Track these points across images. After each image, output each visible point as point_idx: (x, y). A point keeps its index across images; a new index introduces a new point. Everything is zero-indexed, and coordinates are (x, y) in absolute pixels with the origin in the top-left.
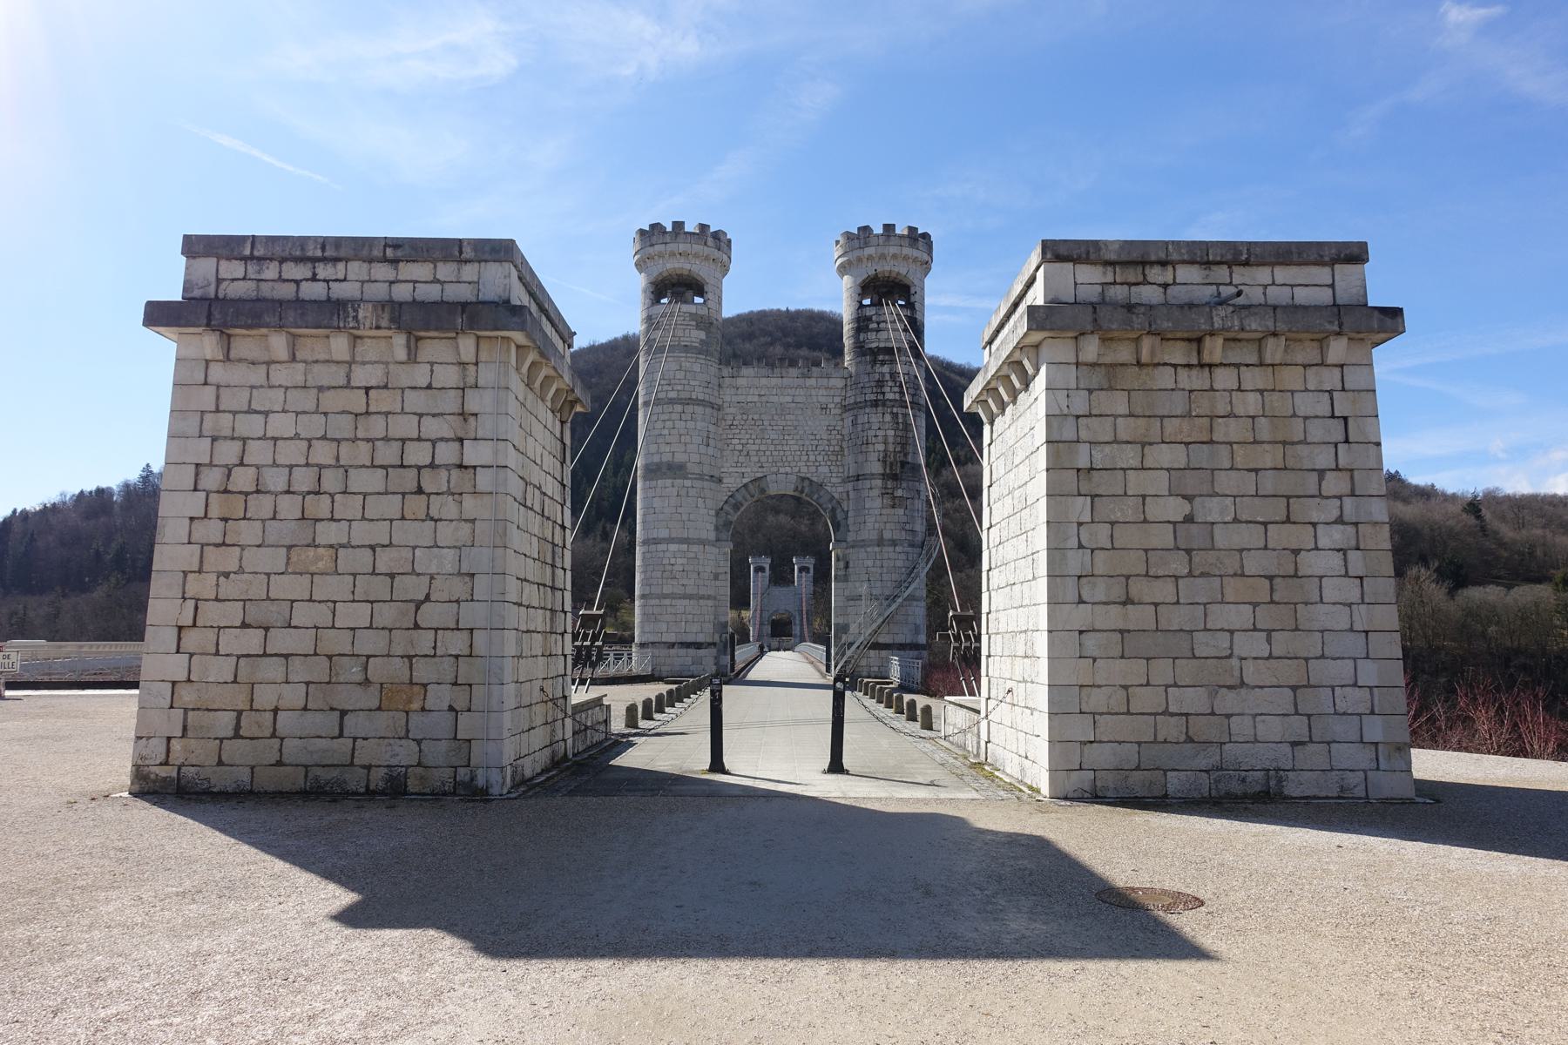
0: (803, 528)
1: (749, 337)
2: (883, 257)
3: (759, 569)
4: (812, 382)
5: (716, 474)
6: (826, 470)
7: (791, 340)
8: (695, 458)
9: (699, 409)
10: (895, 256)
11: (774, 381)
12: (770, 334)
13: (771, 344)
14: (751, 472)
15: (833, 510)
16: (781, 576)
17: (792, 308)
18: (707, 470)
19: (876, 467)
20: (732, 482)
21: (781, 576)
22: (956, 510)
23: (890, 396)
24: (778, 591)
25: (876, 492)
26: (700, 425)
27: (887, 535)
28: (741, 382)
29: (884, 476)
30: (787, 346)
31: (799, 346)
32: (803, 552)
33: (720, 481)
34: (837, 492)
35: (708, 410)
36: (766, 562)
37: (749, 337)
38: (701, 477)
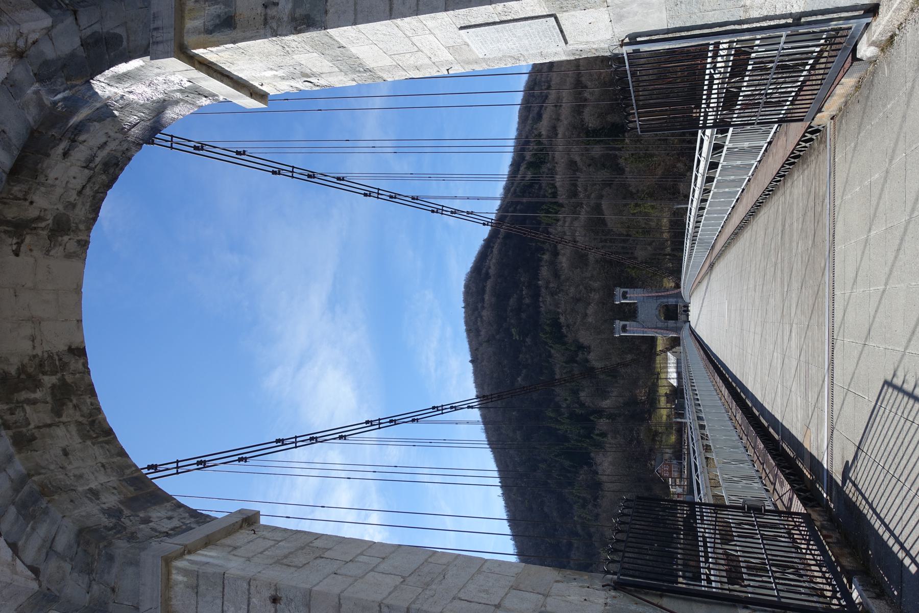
0: (597, 297)
1: (478, 331)
3: (624, 328)
7: (480, 305)
12: (476, 318)
13: (481, 317)
15: (46, 74)
16: (630, 313)
17: (463, 305)
21: (630, 313)
22: (586, 190)
24: (642, 314)
30: (483, 308)
31: (483, 300)
32: (612, 296)
36: (619, 324)
37: (478, 331)
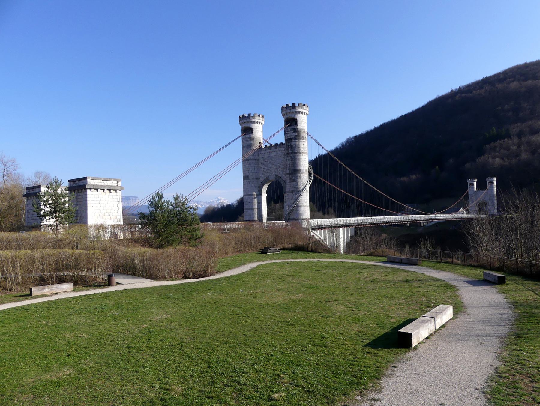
2: (287, 114)
4: (277, 150)
5: (258, 177)
6: (281, 173)
8: (251, 174)
9: (252, 161)
10: (289, 113)
11: (269, 151)
13: (513, 81)
14: (266, 175)
16: (482, 186)
18: (254, 177)
19: (288, 172)
20: (262, 179)
23: (290, 151)
25: (288, 178)
26: (252, 165)
27: (291, 190)
28: (263, 152)
29: (290, 174)
33: (259, 178)
34: (284, 178)
35: (254, 161)
38: (253, 178)
